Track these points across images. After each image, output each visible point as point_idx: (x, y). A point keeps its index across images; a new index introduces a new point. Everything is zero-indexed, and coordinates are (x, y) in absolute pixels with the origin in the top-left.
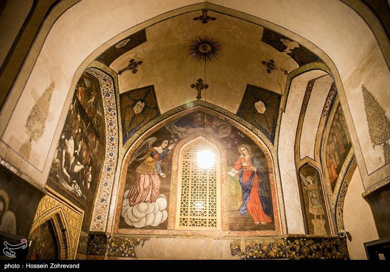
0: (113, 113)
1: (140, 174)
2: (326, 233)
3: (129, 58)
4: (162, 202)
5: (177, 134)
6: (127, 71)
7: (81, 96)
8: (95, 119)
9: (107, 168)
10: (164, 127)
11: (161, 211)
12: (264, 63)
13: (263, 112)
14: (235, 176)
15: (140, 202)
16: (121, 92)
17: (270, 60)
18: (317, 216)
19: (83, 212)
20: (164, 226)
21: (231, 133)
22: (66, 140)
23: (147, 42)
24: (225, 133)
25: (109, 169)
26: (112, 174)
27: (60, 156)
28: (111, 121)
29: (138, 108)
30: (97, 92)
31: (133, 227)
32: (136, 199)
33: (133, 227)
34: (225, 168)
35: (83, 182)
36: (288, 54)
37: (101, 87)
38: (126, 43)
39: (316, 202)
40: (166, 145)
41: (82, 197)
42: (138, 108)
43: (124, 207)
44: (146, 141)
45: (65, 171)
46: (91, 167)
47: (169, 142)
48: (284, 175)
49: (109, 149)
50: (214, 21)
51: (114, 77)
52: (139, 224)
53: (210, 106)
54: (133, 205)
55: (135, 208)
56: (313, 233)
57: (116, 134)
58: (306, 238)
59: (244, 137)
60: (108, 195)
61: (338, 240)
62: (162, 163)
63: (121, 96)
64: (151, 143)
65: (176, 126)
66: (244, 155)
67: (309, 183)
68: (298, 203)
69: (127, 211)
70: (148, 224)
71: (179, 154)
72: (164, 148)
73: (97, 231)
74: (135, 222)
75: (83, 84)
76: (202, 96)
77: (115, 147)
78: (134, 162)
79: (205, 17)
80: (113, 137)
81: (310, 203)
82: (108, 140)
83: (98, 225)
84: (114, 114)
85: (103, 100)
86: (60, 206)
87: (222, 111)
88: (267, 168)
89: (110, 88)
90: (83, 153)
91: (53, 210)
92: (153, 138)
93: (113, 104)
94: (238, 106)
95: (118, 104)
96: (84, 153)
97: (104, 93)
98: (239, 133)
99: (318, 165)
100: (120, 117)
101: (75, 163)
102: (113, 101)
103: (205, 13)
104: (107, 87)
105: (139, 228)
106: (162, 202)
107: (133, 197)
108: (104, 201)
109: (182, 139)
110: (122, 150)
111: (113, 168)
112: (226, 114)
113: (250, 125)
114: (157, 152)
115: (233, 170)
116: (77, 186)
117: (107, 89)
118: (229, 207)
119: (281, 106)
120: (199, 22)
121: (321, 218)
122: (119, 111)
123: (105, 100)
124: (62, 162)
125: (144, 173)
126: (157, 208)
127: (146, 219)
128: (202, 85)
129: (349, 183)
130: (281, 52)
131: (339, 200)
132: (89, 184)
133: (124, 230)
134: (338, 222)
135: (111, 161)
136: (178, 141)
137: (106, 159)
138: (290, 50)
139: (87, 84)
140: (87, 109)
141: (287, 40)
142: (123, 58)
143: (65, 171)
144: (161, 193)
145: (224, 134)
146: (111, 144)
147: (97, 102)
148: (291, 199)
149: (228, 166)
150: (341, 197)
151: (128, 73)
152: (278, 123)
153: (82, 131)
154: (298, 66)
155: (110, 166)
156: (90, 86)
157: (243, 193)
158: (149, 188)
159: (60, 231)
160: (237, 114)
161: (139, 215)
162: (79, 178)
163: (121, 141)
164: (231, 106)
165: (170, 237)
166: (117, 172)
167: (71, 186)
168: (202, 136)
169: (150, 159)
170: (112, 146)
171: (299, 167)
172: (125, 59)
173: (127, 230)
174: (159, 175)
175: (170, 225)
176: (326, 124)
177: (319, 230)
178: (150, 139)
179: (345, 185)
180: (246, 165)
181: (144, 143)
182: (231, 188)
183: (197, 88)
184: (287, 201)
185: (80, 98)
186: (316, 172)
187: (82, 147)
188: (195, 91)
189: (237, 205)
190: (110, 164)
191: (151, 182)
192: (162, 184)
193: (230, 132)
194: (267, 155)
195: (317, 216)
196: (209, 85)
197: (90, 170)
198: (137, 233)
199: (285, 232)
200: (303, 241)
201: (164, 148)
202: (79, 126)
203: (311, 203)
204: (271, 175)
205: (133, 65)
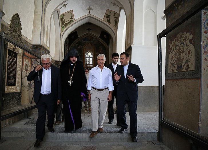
94: (100, 35)
110: (70, 48)
113: (102, 40)
188: (88, 31)
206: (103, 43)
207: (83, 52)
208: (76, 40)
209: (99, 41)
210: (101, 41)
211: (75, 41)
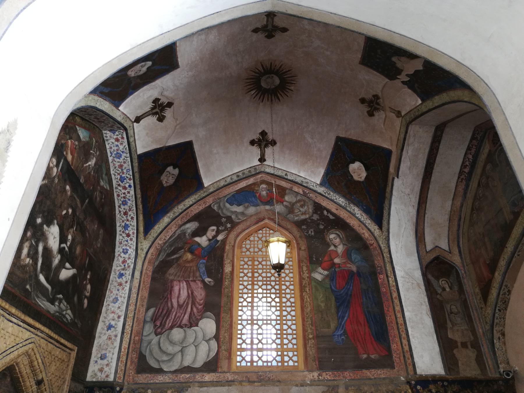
0: (127, 185)
1: (172, 281)
2: (479, 372)
3: (151, 96)
4: (208, 325)
5: (231, 217)
6: (150, 117)
7: (72, 154)
8: (97, 194)
9: (118, 273)
10: (210, 205)
11: (208, 341)
12: (363, 101)
13: (363, 179)
14: (323, 280)
15: (171, 328)
16: (140, 151)
17: (374, 96)
18: (462, 343)
19: (76, 348)
20: (212, 365)
21: (314, 213)
22: (45, 226)
23: (178, 70)
24: (304, 213)
25: (121, 275)
26: (126, 282)
27: (33, 254)
28: (124, 197)
29: (170, 176)
30: (100, 150)
31: (160, 371)
32: (165, 323)
33: (160, 371)
34: (307, 267)
35: (76, 299)
36: (403, 82)
37: (106, 143)
38: (144, 69)
39: (458, 320)
40: (214, 233)
41: (73, 323)
42: (170, 176)
43: (146, 336)
44: (182, 228)
45: (42, 278)
46: (89, 273)
47: (218, 229)
48: (402, 277)
49: (121, 243)
50: (285, 33)
51: (127, 127)
52: (171, 363)
53: (280, 173)
54: (160, 333)
55: (163, 338)
56: (458, 373)
57: (132, 218)
58: (447, 381)
59: (334, 218)
60: (119, 317)
61: (501, 382)
62: (207, 261)
63: (140, 156)
64: (189, 231)
65: (228, 205)
66: (335, 246)
67: (444, 289)
68: (429, 322)
69: (151, 342)
70: (186, 363)
71: (234, 246)
72: (211, 238)
73: (99, 380)
74: (163, 361)
75: (74, 136)
76: (266, 157)
77: (131, 240)
78: (162, 262)
79: (270, 27)
80: (128, 223)
81: (448, 321)
82: (121, 228)
83: (101, 370)
84: (130, 186)
85: (111, 165)
86: (33, 340)
87: (298, 180)
88: (373, 266)
89: (121, 144)
90: (76, 249)
91: (18, 346)
92: (193, 223)
93: (128, 170)
94: (322, 171)
95: (136, 169)
96: (78, 250)
97: (111, 153)
98: (325, 213)
99: (456, 260)
100: (139, 191)
101: (62, 265)
102: (127, 165)
103: (270, 20)
104: (116, 143)
105: (170, 372)
106: (208, 325)
107: (161, 319)
108: (112, 329)
109: (238, 223)
110: (145, 245)
111: (129, 272)
112: (305, 185)
113: (341, 201)
114: (199, 244)
115: (320, 270)
116: (64, 305)
117: (117, 146)
118: (316, 330)
119: (392, 170)
120: (261, 36)
121: (469, 346)
122: (138, 182)
123: (114, 165)
124: (36, 264)
125: (179, 278)
126: (200, 335)
127: (182, 356)
128: (267, 141)
129: (513, 287)
130: (391, 80)
131: (496, 315)
132: (86, 301)
133: (145, 376)
134: (498, 353)
135: (124, 262)
136: (232, 228)
137: (116, 259)
138: (407, 75)
139: (81, 137)
140: (82, 177)
141: (403, 59)
142: (141, 94)
143: (42, 278)
144: (206, 311)
145: (302, 214)
146: (124, 235)
147: (101, 167)
148: (416, 315)
149: (311, 263)
150: (500, 310)
151: (151, 120)
152: (387, 195)
153: (74, 211)
154: (420, 102)
155: (123, 269)
156: (88, 139)
157: (338, 308)
158: (188, 304)
159: (33, 383)
160: (322, 184)
161: (170, 349)
162: (68, 290)
163: (141, 229)
164: (312, 172)
165: (221, 386)
166: (135, 279)
167: (53, 304)
168: (269, 219)
169: (189, 256)
170: (126, 238)
171: (425, 264)
172: (145, 97)
173: (150, 375)
174: (203, 281)
175: (224, 364)
176: (465, 193)
177: (469, 370)
178: (188, 225)
179: (506, 290)
180: (339, 262)
181: (178, 232)
182: (317, 299)
183: (260, 146)
184: (410, 319)
185: (70, 158)
186: (454, 270)
187: (73, 240)
188: (256, 151)
189: (329, 327)
190: (123, 267)
191: (190, 292)
192: (207, 296)
193: (311, 211)
194: (372, 245)
195: (462, 343)
196: (277, 140)
197: (88, 277)
198: (167, 381)
199: (411, 373)
200: (443, 386)
201: (211, 238)
202: (68, 204)
203: (451, 321)
204: (381, 276)
205: (159, 109)
206: (343, 214)
207: (228, 269)
208: (188, 202)
209: (318, 208)
210: (337, 203)
211: (181, 207)
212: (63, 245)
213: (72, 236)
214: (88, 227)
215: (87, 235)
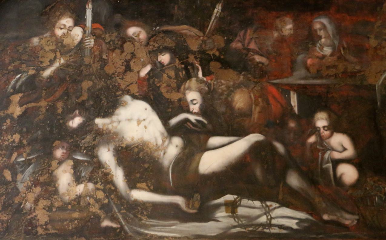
22: (99, 122)
35: (294, 180)
45: (141, 195)
116: (251, 208)
143: (141, 195)
153: (180, 52)
212: (174, 121)
213: (200, 91)
214: (252, 46)
215: (258, 59)
